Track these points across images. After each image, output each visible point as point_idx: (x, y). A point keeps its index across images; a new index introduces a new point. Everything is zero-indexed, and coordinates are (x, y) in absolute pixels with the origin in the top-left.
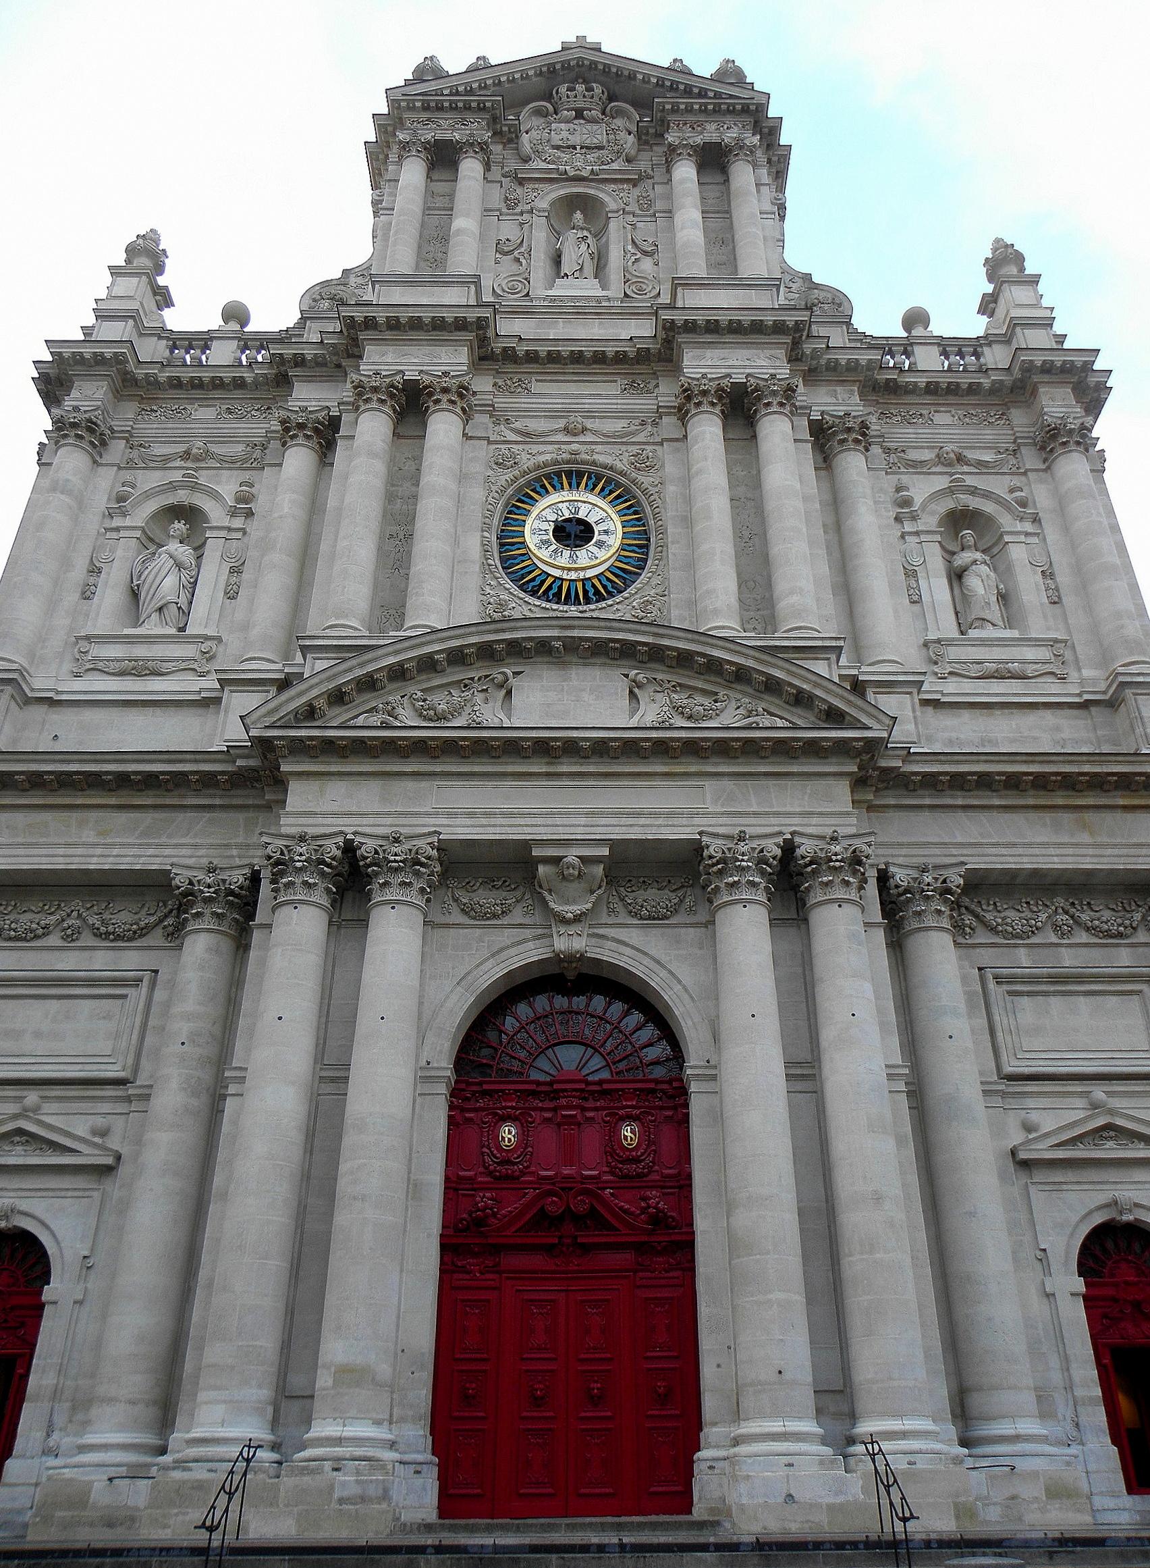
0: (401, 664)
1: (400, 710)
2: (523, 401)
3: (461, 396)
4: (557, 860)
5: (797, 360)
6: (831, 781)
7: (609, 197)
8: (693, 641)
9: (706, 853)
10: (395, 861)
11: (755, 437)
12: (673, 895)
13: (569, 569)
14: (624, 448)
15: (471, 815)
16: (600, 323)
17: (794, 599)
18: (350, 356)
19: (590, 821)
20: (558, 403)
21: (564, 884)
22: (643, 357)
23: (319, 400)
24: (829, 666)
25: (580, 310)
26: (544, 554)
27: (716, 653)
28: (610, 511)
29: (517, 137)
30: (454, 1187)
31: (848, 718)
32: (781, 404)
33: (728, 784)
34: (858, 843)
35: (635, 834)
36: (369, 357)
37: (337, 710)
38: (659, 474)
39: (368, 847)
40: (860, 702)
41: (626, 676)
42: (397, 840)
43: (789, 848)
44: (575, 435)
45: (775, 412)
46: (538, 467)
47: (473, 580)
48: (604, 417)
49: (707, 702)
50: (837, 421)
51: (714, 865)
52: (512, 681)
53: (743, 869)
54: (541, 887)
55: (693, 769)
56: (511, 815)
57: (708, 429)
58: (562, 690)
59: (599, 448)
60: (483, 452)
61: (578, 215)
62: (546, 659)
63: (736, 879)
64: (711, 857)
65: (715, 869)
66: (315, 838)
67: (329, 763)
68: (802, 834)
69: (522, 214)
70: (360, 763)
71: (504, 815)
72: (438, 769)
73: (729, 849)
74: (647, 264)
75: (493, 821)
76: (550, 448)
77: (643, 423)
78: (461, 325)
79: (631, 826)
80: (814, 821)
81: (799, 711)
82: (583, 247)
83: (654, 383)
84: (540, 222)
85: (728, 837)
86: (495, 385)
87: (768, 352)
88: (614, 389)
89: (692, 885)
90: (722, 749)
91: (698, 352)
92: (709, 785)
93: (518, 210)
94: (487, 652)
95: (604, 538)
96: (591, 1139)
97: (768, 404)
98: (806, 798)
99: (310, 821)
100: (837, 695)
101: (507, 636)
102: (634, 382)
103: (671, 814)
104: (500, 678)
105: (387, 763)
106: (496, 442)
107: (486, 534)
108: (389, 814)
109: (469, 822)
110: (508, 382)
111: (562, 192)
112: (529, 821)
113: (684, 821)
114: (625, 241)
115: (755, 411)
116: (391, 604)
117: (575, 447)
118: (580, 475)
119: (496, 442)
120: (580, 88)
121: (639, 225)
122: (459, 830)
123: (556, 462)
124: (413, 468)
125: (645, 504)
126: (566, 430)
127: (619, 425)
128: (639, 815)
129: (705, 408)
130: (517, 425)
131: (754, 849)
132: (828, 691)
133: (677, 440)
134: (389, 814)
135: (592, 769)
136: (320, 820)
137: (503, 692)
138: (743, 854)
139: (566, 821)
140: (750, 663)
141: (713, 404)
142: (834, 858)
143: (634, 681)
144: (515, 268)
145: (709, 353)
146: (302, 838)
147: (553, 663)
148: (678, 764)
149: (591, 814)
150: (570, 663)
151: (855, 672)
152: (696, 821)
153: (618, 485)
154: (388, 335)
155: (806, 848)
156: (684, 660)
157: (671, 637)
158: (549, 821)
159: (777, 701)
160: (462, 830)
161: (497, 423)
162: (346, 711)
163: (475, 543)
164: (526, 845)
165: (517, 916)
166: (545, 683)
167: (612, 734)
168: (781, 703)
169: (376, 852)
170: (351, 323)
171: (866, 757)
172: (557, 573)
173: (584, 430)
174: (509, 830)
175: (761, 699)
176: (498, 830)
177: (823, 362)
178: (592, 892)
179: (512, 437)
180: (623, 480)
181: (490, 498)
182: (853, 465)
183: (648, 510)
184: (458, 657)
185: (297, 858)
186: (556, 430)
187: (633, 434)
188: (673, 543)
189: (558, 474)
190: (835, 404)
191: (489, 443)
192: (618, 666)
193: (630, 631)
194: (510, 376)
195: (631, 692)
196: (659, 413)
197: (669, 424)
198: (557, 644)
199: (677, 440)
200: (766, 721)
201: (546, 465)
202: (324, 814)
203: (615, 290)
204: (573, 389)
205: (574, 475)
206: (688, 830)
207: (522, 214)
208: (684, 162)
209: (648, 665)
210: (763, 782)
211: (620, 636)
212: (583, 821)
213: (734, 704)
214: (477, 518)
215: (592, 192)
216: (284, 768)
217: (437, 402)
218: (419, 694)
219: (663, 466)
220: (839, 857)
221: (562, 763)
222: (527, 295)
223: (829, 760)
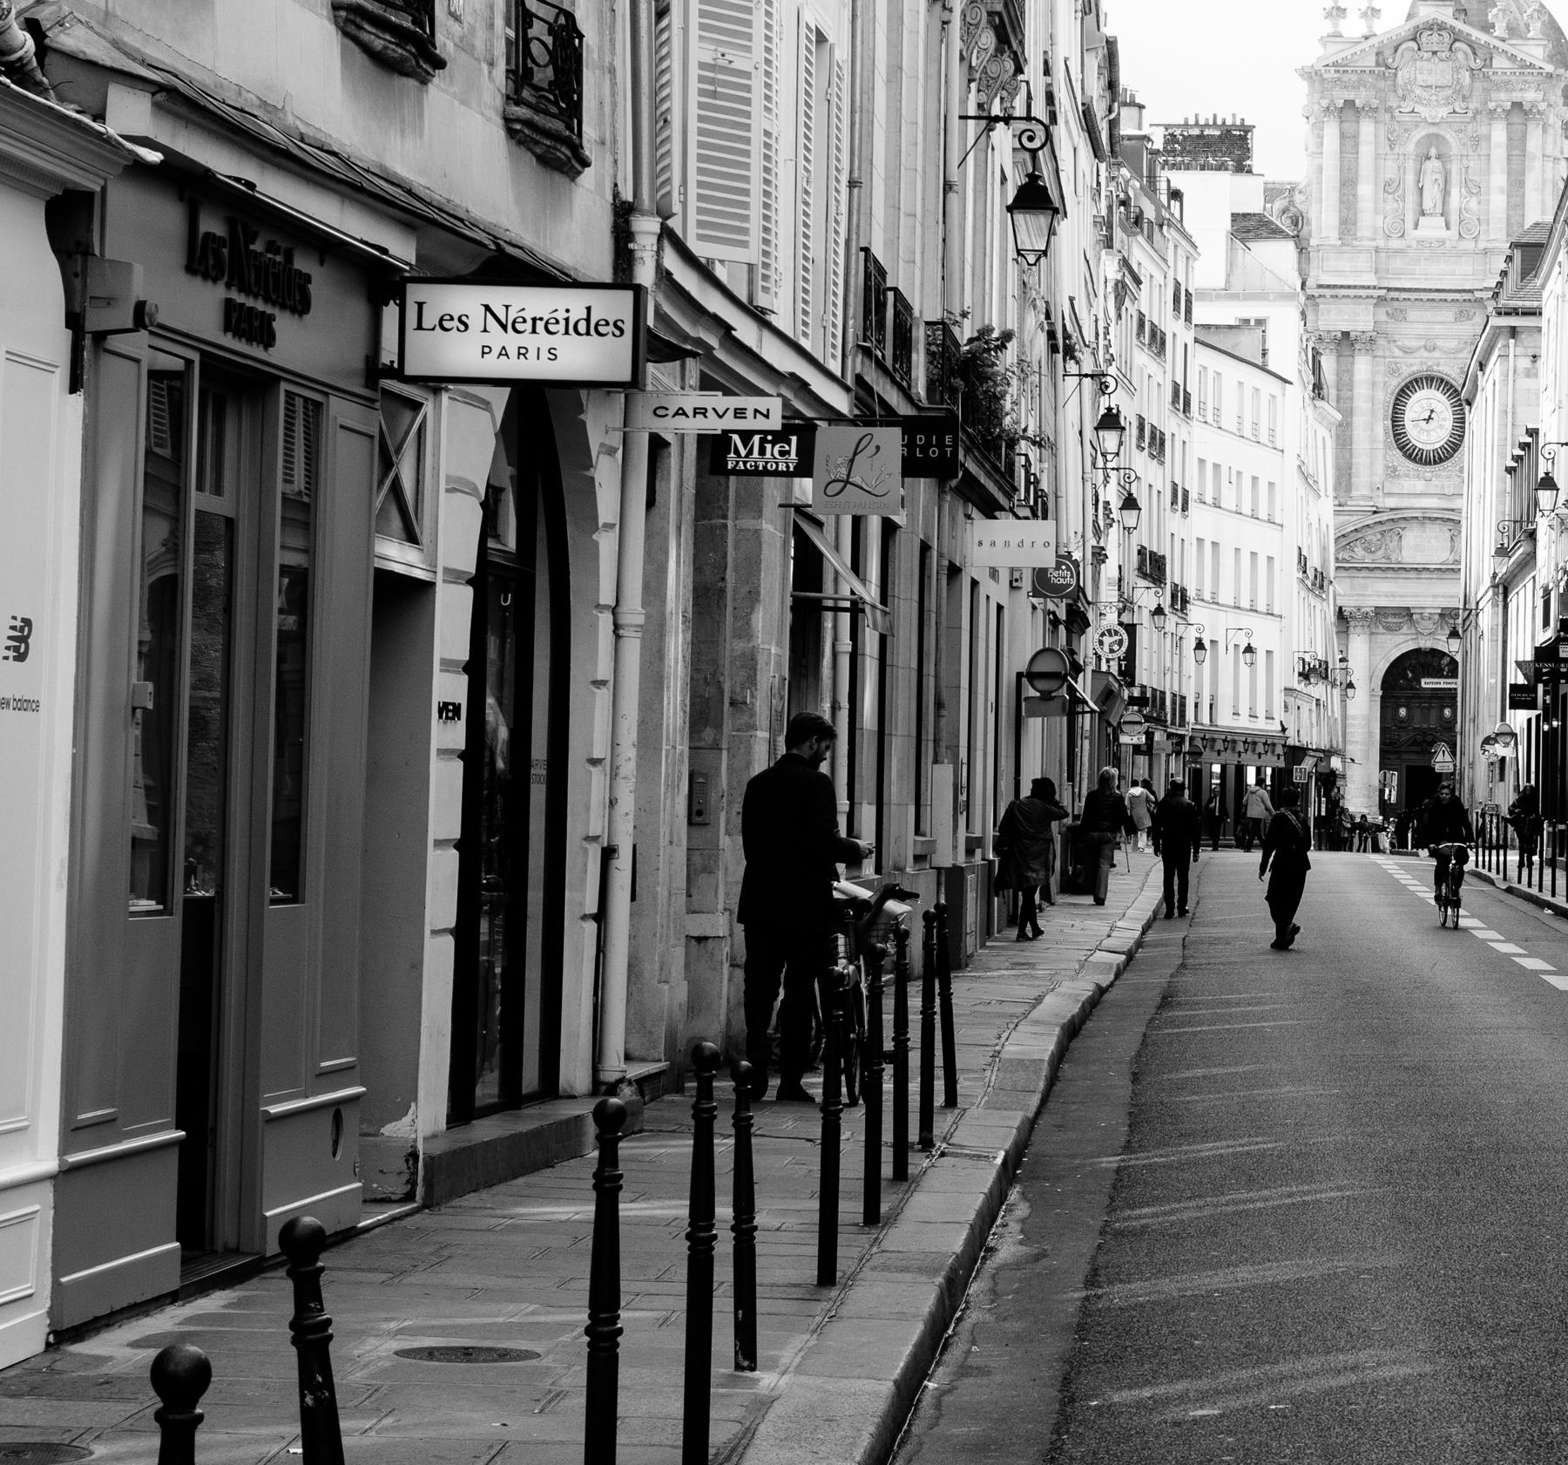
20: (1420, 329)
25: (1434, 249)
29: (1396, 75)
30: (1384, 730)
47: (1380, 454)
74: (1474, 201)
96: (1434, 714)
111: (1423, 133)
120: (1435, 37)
127: (1453, 344)
160: (1383, 602)
164: (1408, 609)
165: (1405, 630)
172: (1420, 446)
179: (1398, 353)
205: (1431, 380)
215: (1442, 133)
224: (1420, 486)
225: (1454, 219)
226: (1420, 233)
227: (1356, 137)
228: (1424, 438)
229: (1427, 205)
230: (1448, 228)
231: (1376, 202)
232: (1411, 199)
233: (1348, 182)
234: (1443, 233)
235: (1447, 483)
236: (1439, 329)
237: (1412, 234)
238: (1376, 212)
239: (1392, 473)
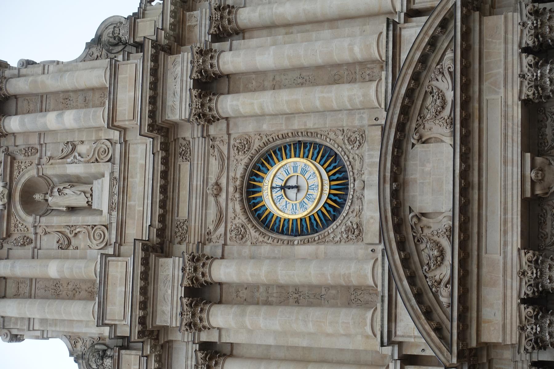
0: (408, 278)
1: (437, 278)
2: (195, 224)
3: (198, 260)
4: (533, 183)
5: (170, 49)
6: (484, 27)
7: (27, 174)
8: (395, 105)
9: (531, 97)
10: (537, 273)
11: (228, 76)
12: (550, 119)
13: (322, 190)
14: (232, 158)
15: (505, 232)
16: (132, 177)
17: (357, 49)
18: (157, 339)
19: (510, 164)
20: (196, 202)
21: (546, 179)
22: (165, 147)
23: (187, 359)
24: (405, 28)
26: (310, 206)
27: (403, 91)
28: (280, 165)
31: (447, 16)
32: (212, 58)
33: (485, 85)
34: (525, 12)
35: (517, 138)
36: (165, 321)
37: (435, 316)
38: (252, 135)
39: (526, 290)
40: (439, 9)
41: (413, 145)
42: (524, 273)
43: (526, 50)
44: (221, 189)
45: (218, 61)
46: (245, 212)
47: (332, 248)
48: (208, 172)
49: (430, 99)
50: (214, 25)
51: (538, 93)
52: (417, 211)
53: (541, 76)
54: (547, 193)
55: (477, 105)
56: (505, 209)
57: (227, 104)
58: (423, 183)
59: (232, 174)
60: (233, 248)
61: (38, 197)
62: (401, 194)
63: (548, 80)
64: (534, 94)
65: (541, 92)
66: (521, 322)
67: (471, 318)
68: (520, 43)
69: (36, 234)
70: (471, 299)
71: (505, 213)
72: (475, 253)
73: (529, 84)
74: (82, 149)
75: (509, 220)
76: (230, 205)
77: (213, 147)
78: (145, 262)
79: (513, 140)
80: (510, 36)
81: (439, 45)
82: (66, 191)
83: (181, 141)
84: (44, 220)
85: (521, 83)
86: (180, 243)
87: (170, 66)
88: (185, 167)
89: (544, 108)
90: (466, 87)
91: (168, 111)
92: (485, 97)
93: (33, 237)
94: (398, 227)
95: (299, 170)
97: (212, 65)
98: (494, 41)
99: (508, 327)
100: (433, 22)
101: (389, 214)
102: (180, 154)
103: (506, 117)
104: (415, 220)
105: (471, 284)
106: (225, 240)
107: (296, 242)
108: (505, 281)
109: (510, 234)
110: (178, 234)
111: (19, 207)
112: (509, 199)
113: (510, 110)
114: (63, 163)
115: (214, 74)
116: (352, 296)
117: (231, 189)
118: (249, 186)
119: (225, 240)
121: (49, 154)
122: (515, 238)
123: (242, 201)
124: (244, 291)
125: (274, 144)
126: (216, 196)
128: (506, 136)
129: (213, 105)
130: (212, 228)
131: (529, 70)
132: (430, 26)
133: (228, 125)
134: (505, 281)
135: (476, 163)
136: (508, 321)
137: (423, 218)
138: (533, 76)
139: (510, 178)
140: (410, 72)
141: (210, 100)
142: (535, 25)
143: (418, 140)
144: (80, 236)
145: (169, 103)
146: (522, 328)
147: (404, 190)
148: (473, 113)
149: (505, 163)
150: (404, 179)
151: (402, 15)
152: (510, 102)
153: (259, 161)
154: (150, 310)
155: (529, 41)
156: (405, 111)
157: (392, 118)
158: (509, 187)
159: (432, 57)
160: (515, 238)
161: (210, 240)
162: (436, 310)
163: (302, 249)
166: (417, 194)
167: (458, 150)
168: (433, 55)
169: (531, 285)
170: (141, 333)
171: (470, 7)
172: (325, 197)
173: (217, 184)
174: (515, 210)
175: (430, 66)
176: (515, 217)
177: (172, 33)
178: (550, 164)
179: (221, 230)
180: (255, 159)
181: (268, 242)
182: (246, 16)
183: (278, 142)
184: (402, 245)
185: (534, 331)
186: (217, 202)
187: (221, 153)
188: (306, 125)
189: (249, 200)
190: (201, 26)
191: (225, 244)
192: (406, 151)
193: (388, 142)
194: (173, 234)
195: (424, 143)
196: (206, 136)
197: (213, 130)
198: (394, 186)
199: (228, 125)
200: (447, 62)
201: (243, 208)
202: (504, 318)
203: (106, 168)
204: (184, 193)
206: (515, 108)
207: (36, 234)
208: (5, 124)
209: (407, 133)
210: (484, 66)
211: (390, 148)
212: (509, 168)
213: (434, 83)
214: (284, 249)
215: (19, 187)
216: (474, 344)
217: (203, 275)
218: (426, 267)
219: (246, 134)
220: (535, 22)
221: (473, 181)
222: (106, 226)
223: (472, 28)
224: (371, 195)
225: (94, 169)
226: (105, 209)
227: (19, 281)
228: (316, 194)
229: (81, 201)
230: (103, 176)
231: (75, 258)
232: (74, 219)
233: (57, 291)
234: (106, 180)
235: (367, 160)
236: (197, 182)
237: (104, 218)
238: (83, 258)
239: (356, 232)
